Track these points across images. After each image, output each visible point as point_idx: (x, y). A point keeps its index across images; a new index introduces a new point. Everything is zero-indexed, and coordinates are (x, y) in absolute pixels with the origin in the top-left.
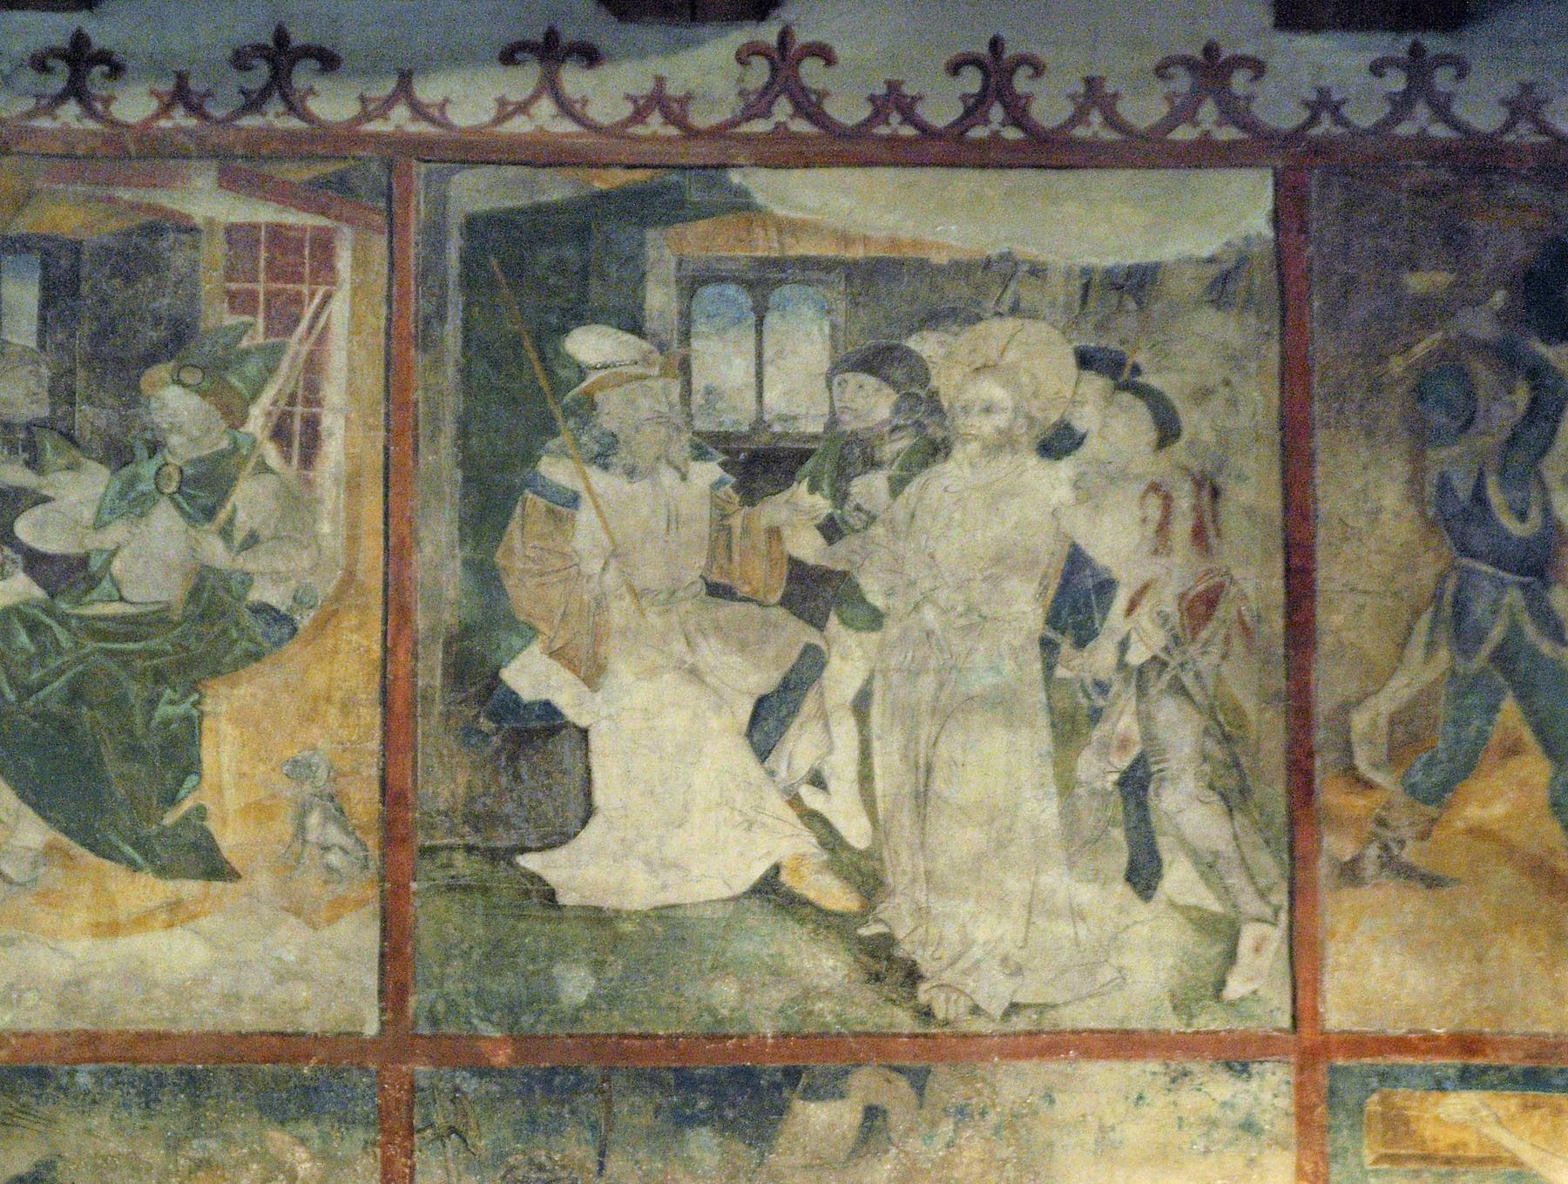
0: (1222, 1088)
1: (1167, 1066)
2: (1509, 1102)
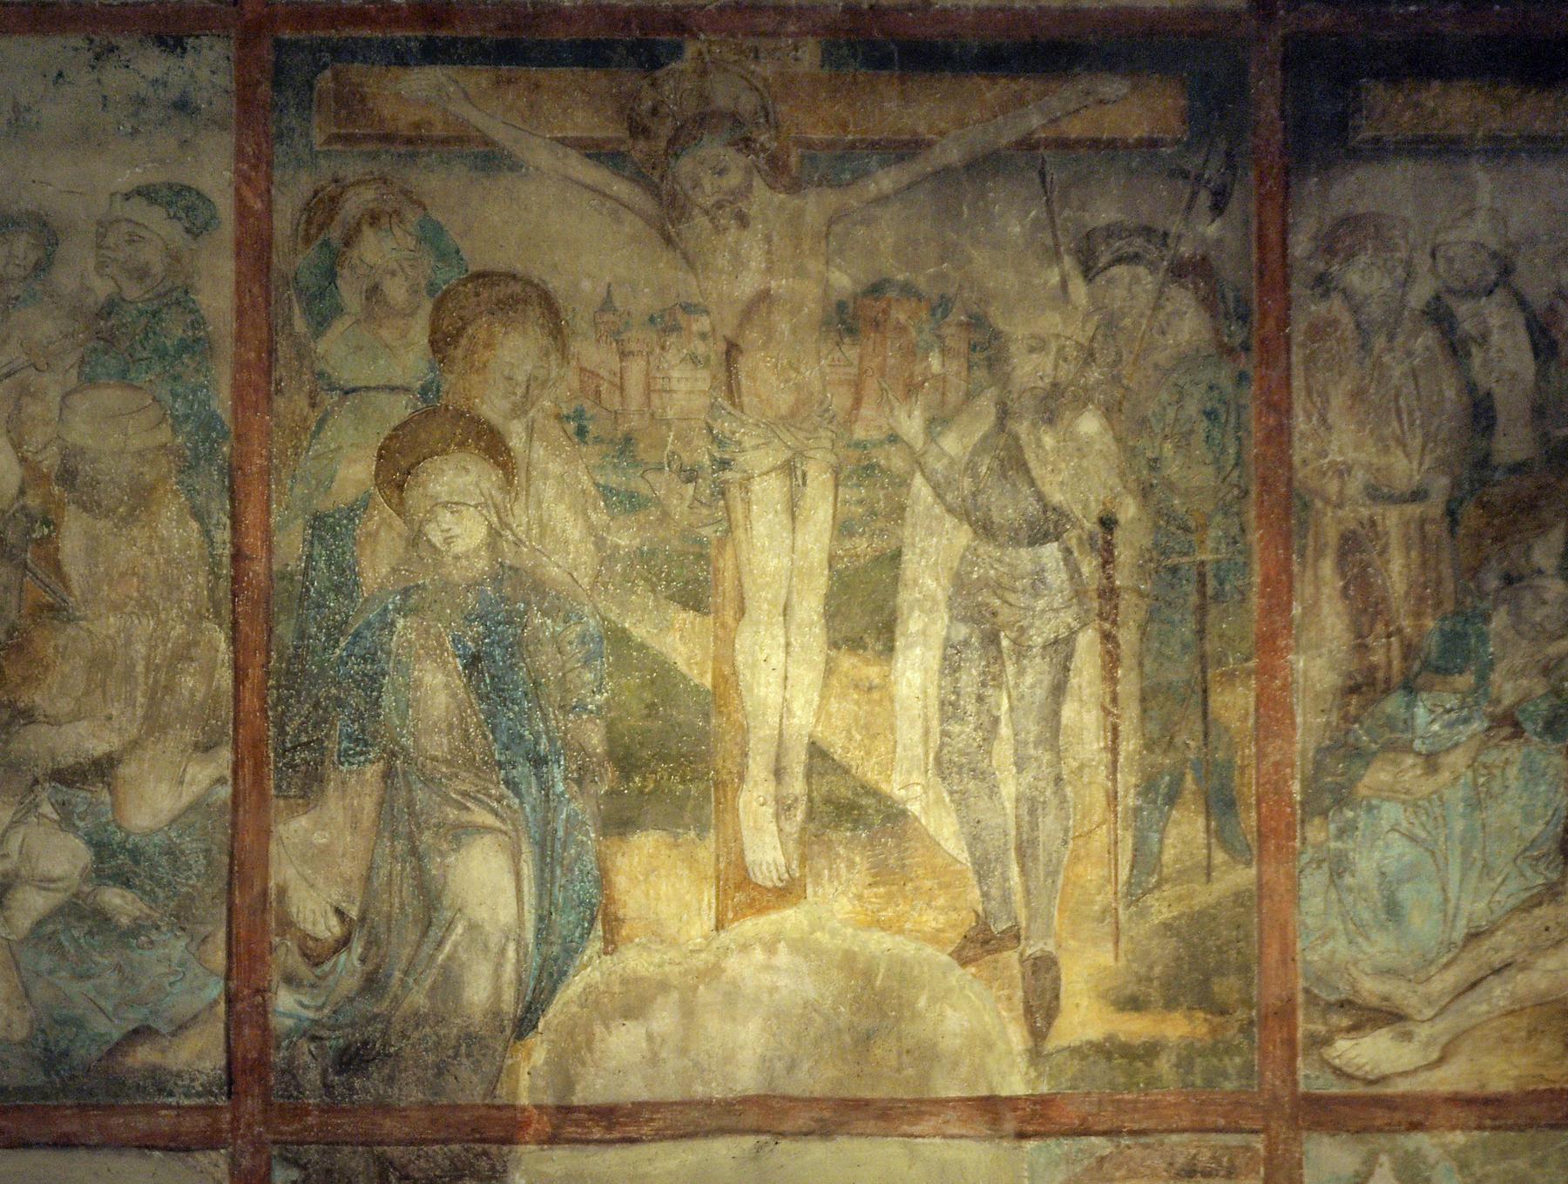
0: (154, 64)
1: (92, 41)
2: (479, 78)
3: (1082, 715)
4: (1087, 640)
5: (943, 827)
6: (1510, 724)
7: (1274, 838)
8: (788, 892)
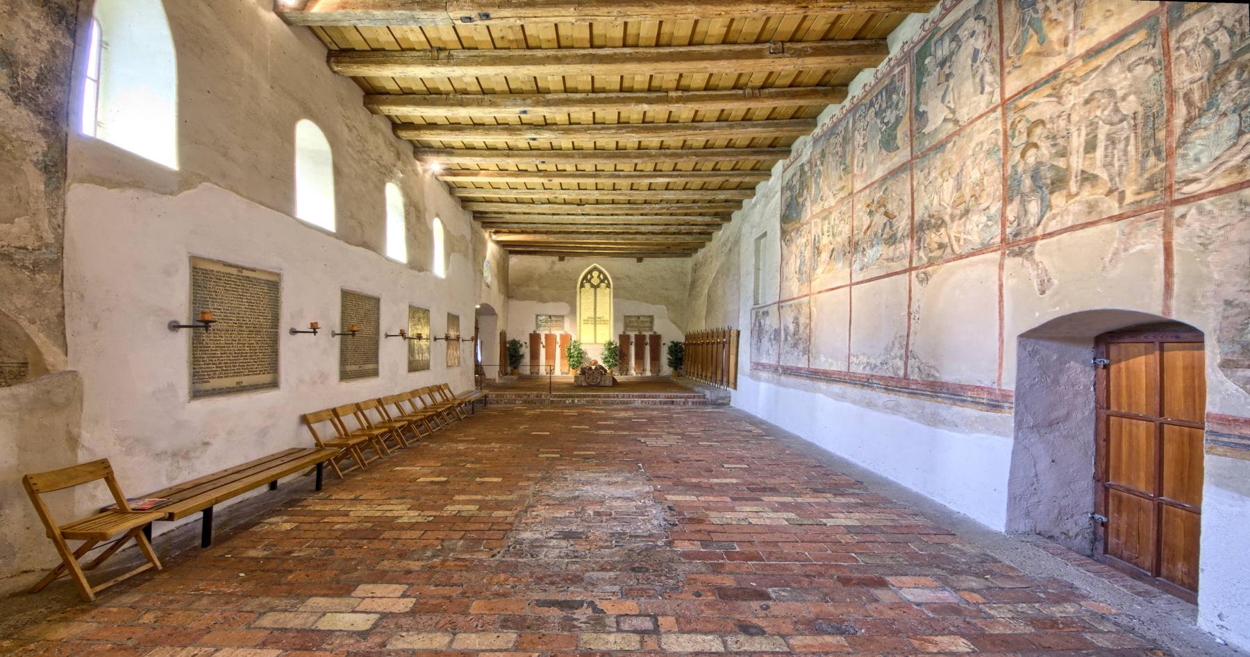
3: (1131, 148)
4: (1132, 135)
5: (1104, 175)
6: (1225, 114)
7: (1170, 154)
8: (1077, 194)
